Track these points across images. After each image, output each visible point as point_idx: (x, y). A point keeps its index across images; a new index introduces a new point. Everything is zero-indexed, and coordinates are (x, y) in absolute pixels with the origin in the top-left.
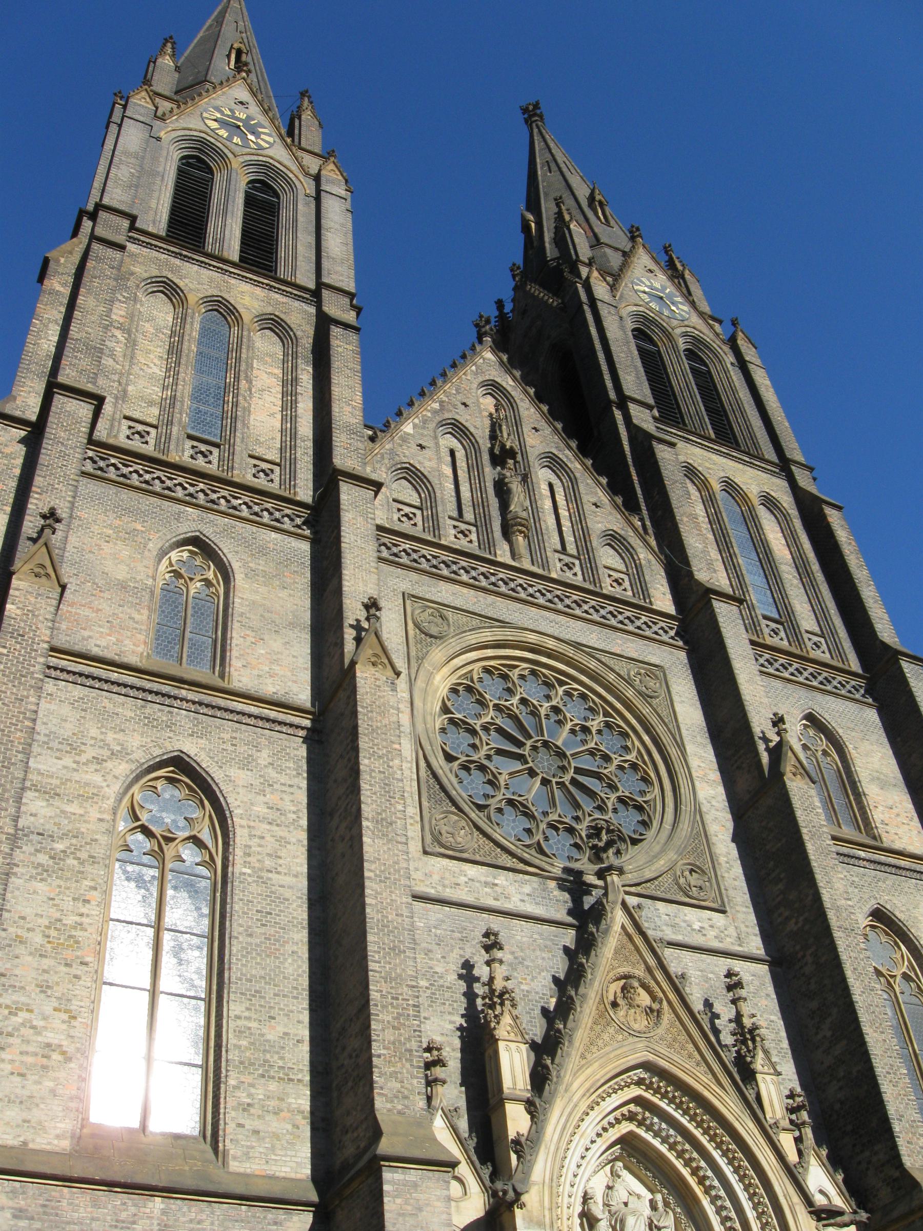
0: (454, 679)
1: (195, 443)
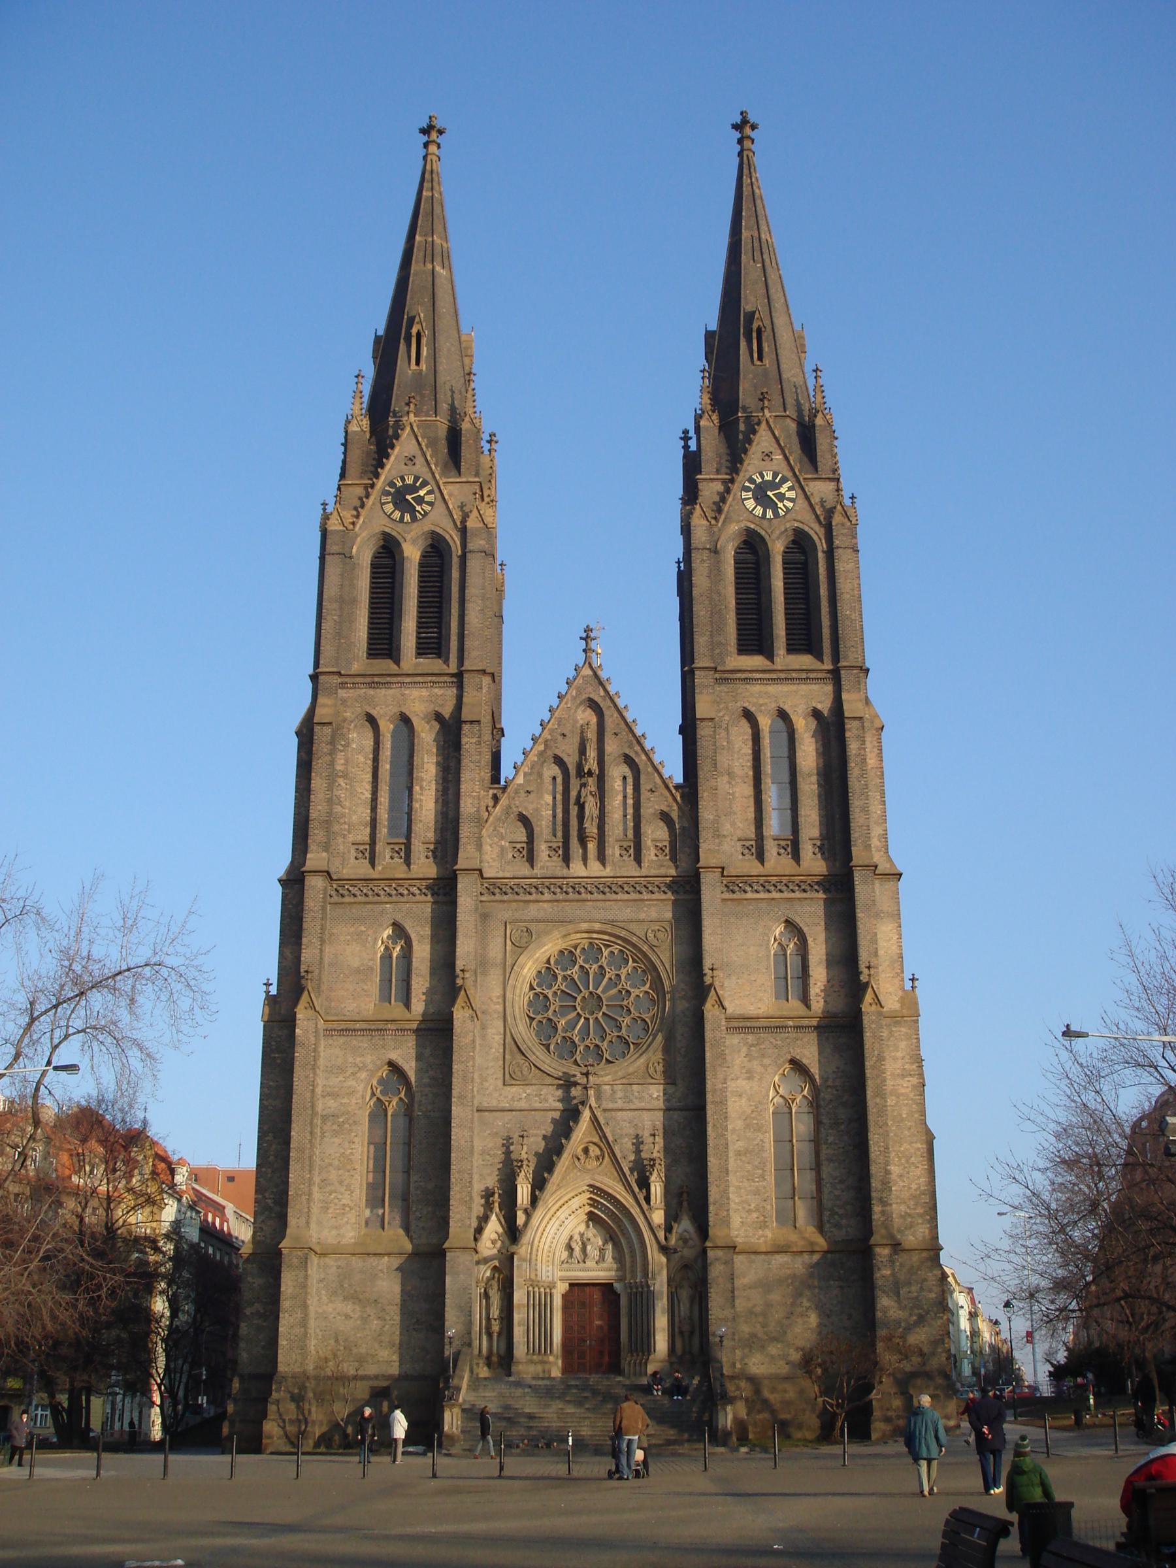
1: (392, 846)
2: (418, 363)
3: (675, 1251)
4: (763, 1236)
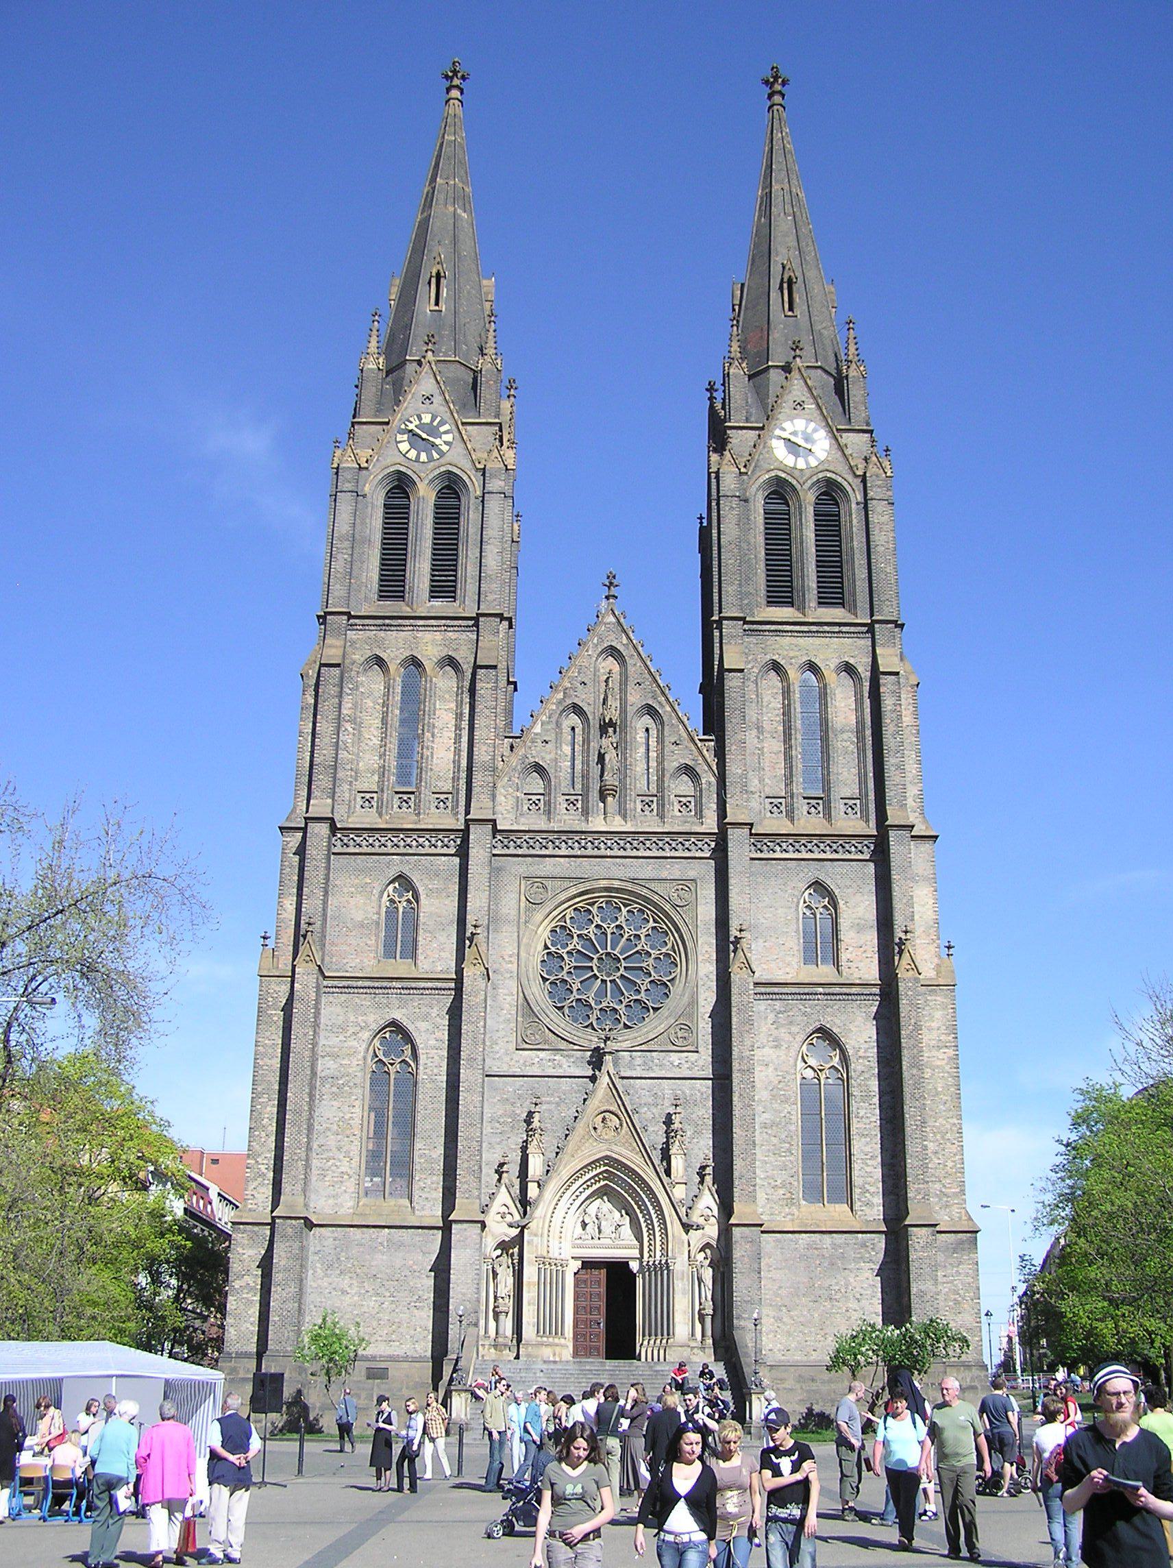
0: (553, 924)
1: (400, 796)
2: (437, 304)
3: (699, 1227)
4: (790, 1214)
